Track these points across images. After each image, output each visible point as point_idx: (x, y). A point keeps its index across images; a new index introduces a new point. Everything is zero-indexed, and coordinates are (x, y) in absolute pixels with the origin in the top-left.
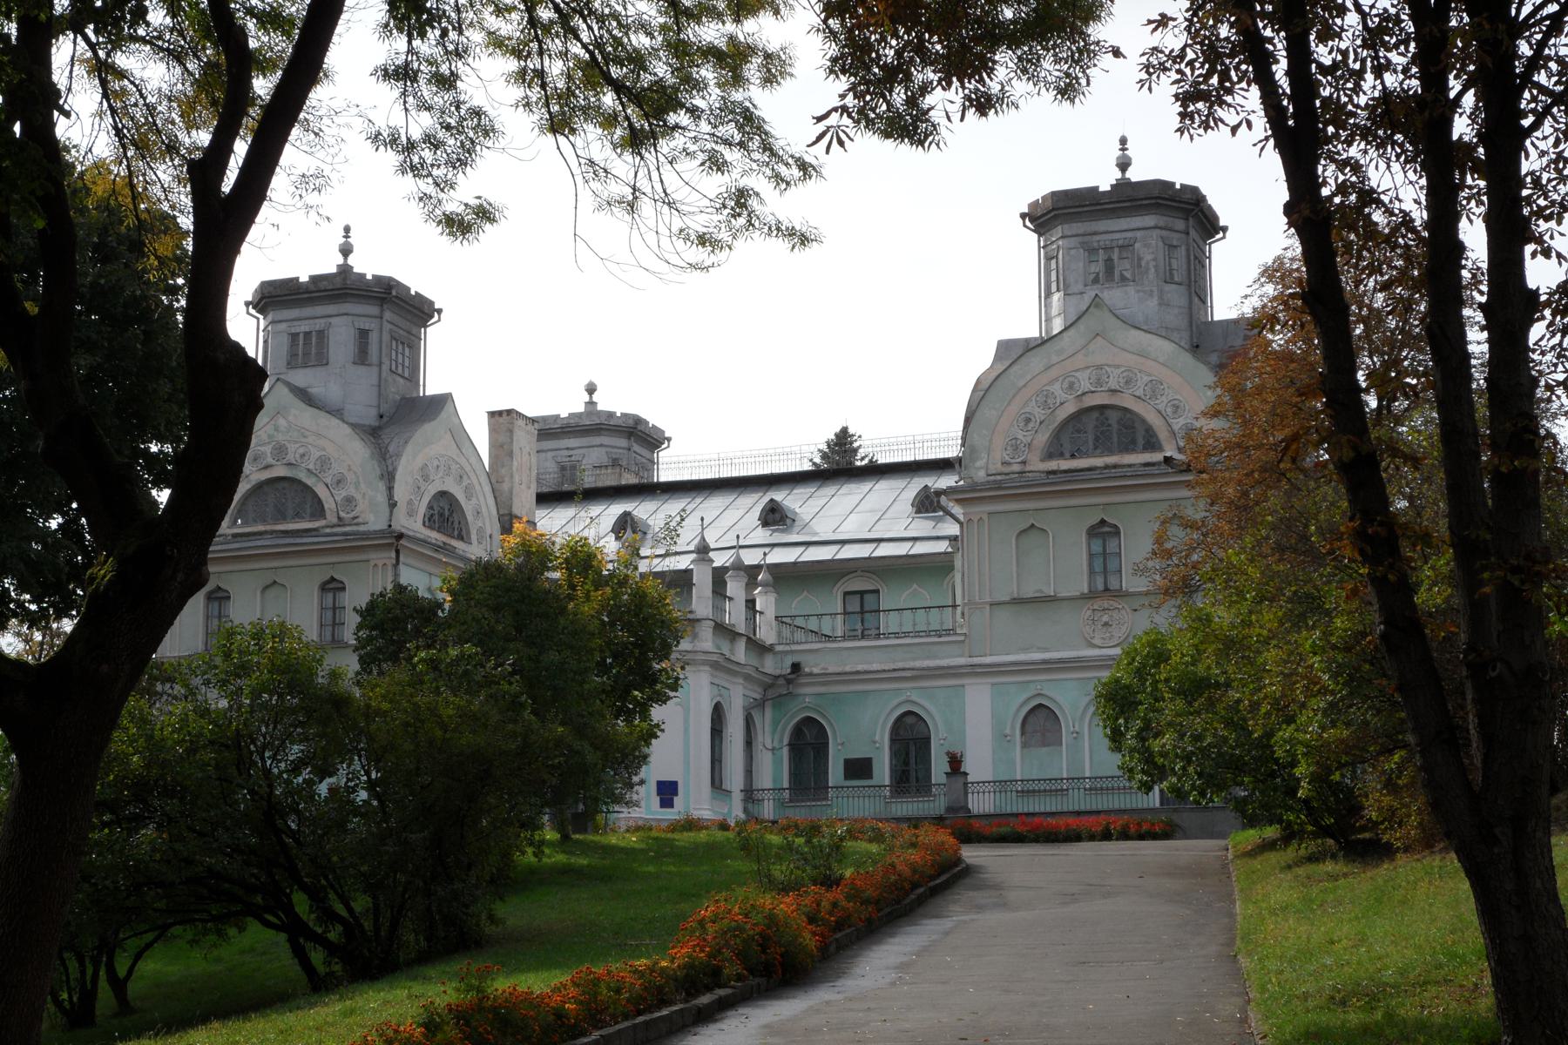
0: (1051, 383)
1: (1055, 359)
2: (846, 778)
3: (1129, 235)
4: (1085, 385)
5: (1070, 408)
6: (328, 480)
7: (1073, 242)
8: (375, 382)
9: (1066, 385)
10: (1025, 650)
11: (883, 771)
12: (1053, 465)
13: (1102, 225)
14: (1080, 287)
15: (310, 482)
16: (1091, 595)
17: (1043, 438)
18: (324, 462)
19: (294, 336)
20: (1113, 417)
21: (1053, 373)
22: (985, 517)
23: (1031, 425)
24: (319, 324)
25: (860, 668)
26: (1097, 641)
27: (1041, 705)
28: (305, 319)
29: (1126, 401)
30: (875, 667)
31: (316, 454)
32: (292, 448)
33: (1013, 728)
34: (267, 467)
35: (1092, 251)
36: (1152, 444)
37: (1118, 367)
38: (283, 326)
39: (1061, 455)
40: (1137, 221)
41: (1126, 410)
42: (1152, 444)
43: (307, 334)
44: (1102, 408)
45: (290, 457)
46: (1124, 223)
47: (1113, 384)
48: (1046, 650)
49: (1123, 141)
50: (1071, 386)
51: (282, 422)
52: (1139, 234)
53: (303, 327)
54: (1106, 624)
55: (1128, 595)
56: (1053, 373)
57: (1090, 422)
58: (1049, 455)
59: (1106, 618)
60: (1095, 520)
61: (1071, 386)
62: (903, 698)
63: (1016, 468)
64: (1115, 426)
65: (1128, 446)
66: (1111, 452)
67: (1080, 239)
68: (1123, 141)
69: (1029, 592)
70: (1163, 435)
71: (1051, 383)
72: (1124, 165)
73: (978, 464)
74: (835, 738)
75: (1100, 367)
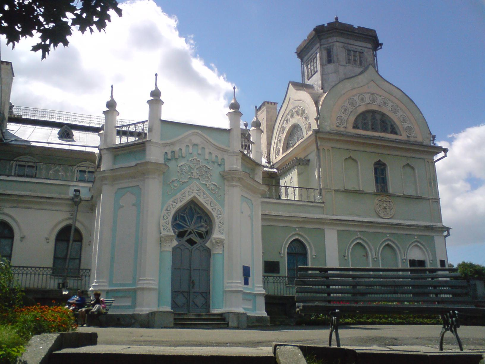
0: (354, 96)
3: (362, 48)
4: (367, 101)
5: (362, 109)
9: (360, 98)
10: (350, 215)
11: (284, 270)
13: (352, 42)
14: (344, 63)
16: (375, 194)
17: (352, 119)
20: (378, 117)
22: (330, 149)
25: (273, 213)
26: (382, 215)
29: (386, 112)
30: (280, 214)
36: (394, 131)
39: (358, 128)
40: (365, 45)
41: (383, 115)
42: (394, 131)
44: (374, 112)
46: (360, 43)
48: (360, 216)
50: (362, 99)
52: (366, 49)
54: (385, 208)
58: (355, 127)
59: (385, 205)
60: (376, 160)
61: (362, 99)
62: (296, 232)
63: (342, 129)
64: (379, 122)
65: (385, 131)
66: (377, 131)
67: (344, 45)
69: (350, 188)
71: (354, 96)
73: (326, 124)
75: (373, 94)
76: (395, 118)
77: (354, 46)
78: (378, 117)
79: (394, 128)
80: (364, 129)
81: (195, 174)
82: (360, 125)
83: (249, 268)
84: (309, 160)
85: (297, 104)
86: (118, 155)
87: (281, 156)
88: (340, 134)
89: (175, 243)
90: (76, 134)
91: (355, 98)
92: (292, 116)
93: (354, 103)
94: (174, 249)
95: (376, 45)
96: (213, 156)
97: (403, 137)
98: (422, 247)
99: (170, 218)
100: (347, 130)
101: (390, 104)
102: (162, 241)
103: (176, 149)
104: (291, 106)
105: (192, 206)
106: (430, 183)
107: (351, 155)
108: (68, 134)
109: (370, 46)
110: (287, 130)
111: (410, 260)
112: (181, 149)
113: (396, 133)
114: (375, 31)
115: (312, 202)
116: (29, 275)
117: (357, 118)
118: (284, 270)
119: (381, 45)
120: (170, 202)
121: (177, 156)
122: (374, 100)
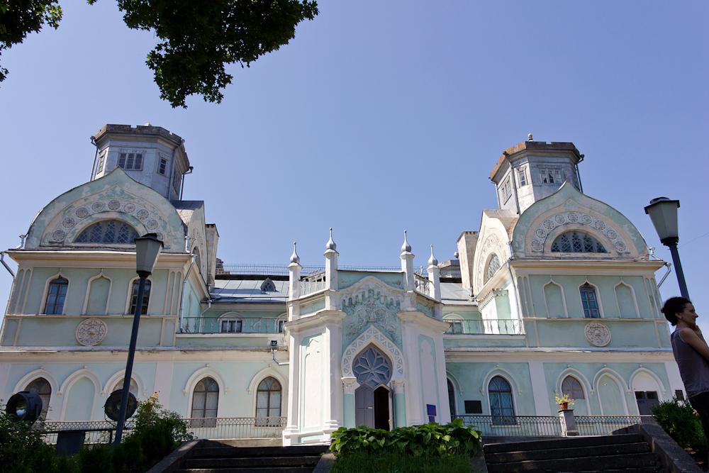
1: (551, 206)
2: (467, 412)
3: (558, 164)
4: (567, 220)
5: (561, 230)
6: (146, 223)
8: (167, 185)
11: (486, 409)
12: (558, 254)
13: (547, 159)
15: (132, 223)
17: (550, 242)
18: (143, 213)
19: (123, 155)
20: (581, 237)
22: (528, 277)
23: (543, 235)
24: (139, 151)
26: (595, 343)
27: (569, 376)
28: (131, 147)
31: (138, 207)
32: (123, 203)
33: (559, 389)
34: (104, 212)
36: (601, 250)
37: (581, 213)
38: (117, 149)
39: (558, 251)
40: (561, 160)
43: (131, 155)
44: (575, 232)
45: (121, 208)
46: (555, 160)
47: (580, 220)
51: (118, 189)
52: (563, 165)
53: (130, 151)
54: (598, 335)
55: (606, 322)
58: (553, 251)
59: (597, 332)
62: (497, 368)
64: (582, 241)
70: (606, 246)
74: (458, 388)
75: (572, 213)
76: (600, 237)
77: (549, 164)
79: (602, 246)
81: (372, 318)
82: (560, 248)
83: (435, 406)
84: (508, 291)
85: (492, 232)
86: (303, 306)
87: (483, 287)
88: (537, 258)
90: (277, 284)
92: (489, 245)
93: (551, 226)
94: (357, 391)
95: (577, 157)
96: (389, 299)
98: (614, 378)
99: (351, 363)
100: (545, 255)
103: (354, 295)
104: (487, 235)
105: (372, 348)
106: (652, 302)
107: (552, 280)
108: (270, 287)
109: (567, 160)
110: (485, 260)
111: (636, 393)
112: (357, 296)
113: (604, 251)
114: (571, 144)
115: (512, 335)
116: (224, 426)
117: (555, 240)
118: (486, 409)
119: (583, 156)
120: (350, 347)
121: (354, 302)
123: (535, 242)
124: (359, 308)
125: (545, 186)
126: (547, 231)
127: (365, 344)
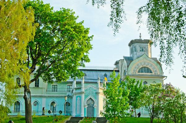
5: (141, 67)
7: (138, 46)
12: (139, 73)
17: (138, 70)
21: (139, 62)
35: (141, 47)
36: (151, 72)
42: (151, 72)
46: (144, 44)
49: (140, 34)
56: (139, 62)
57: (143, 69)
58: (138, 72)
65: (148, 72)
68: (140, 34)
70: (153, 71)
72: (140, 37)
73: (130, 72)
78: (146, 68)
80: (142, 72)
88: (133, 75)
89: (87, 106)
91: (139, 64)
97: (153, 74)
101: (150, 64)
102: (84, 106)
122: (145, 64)
123: (134, 70)
124: (88, 91)
125: (141, 52)
126: (137, 67)
127: (89, 98)
